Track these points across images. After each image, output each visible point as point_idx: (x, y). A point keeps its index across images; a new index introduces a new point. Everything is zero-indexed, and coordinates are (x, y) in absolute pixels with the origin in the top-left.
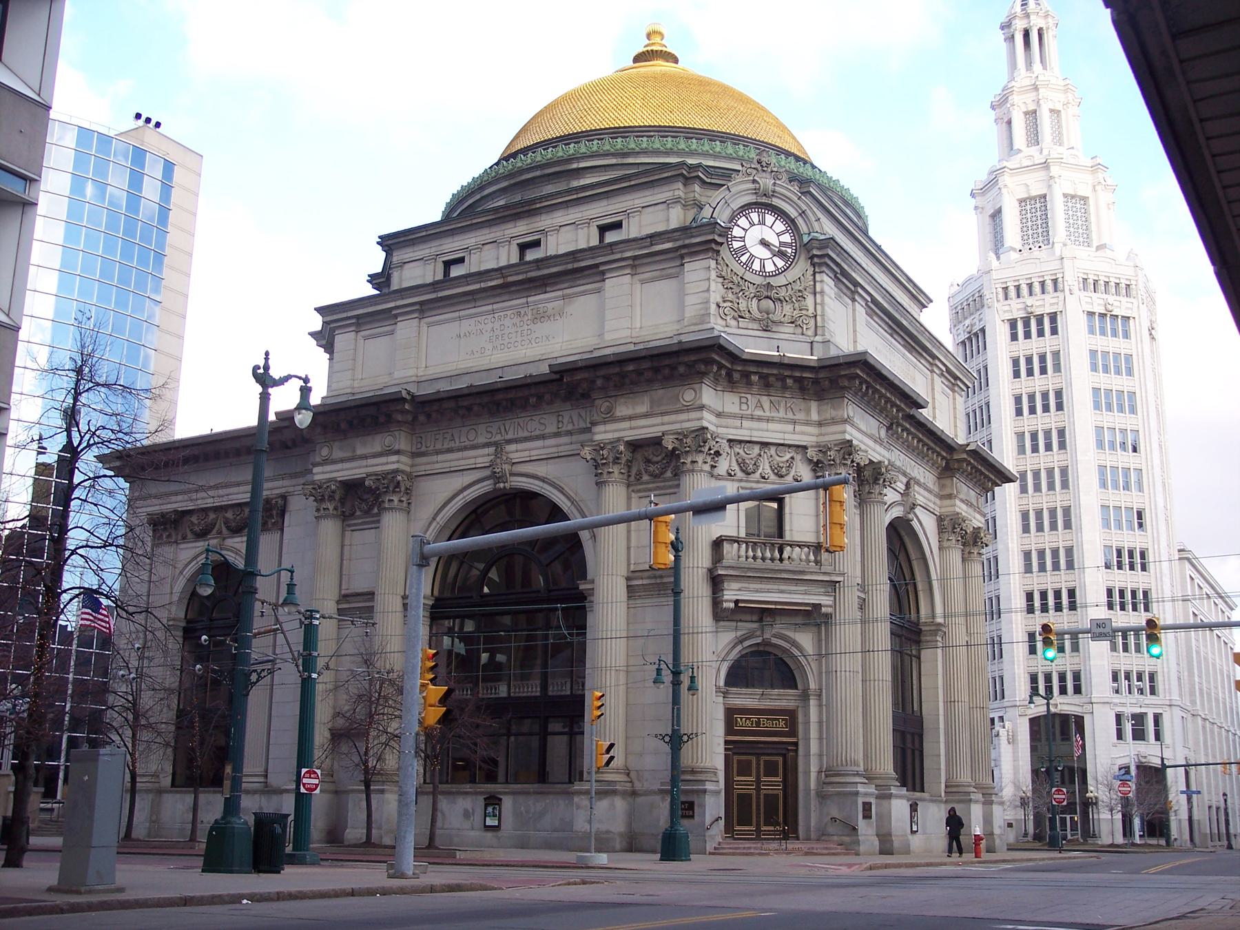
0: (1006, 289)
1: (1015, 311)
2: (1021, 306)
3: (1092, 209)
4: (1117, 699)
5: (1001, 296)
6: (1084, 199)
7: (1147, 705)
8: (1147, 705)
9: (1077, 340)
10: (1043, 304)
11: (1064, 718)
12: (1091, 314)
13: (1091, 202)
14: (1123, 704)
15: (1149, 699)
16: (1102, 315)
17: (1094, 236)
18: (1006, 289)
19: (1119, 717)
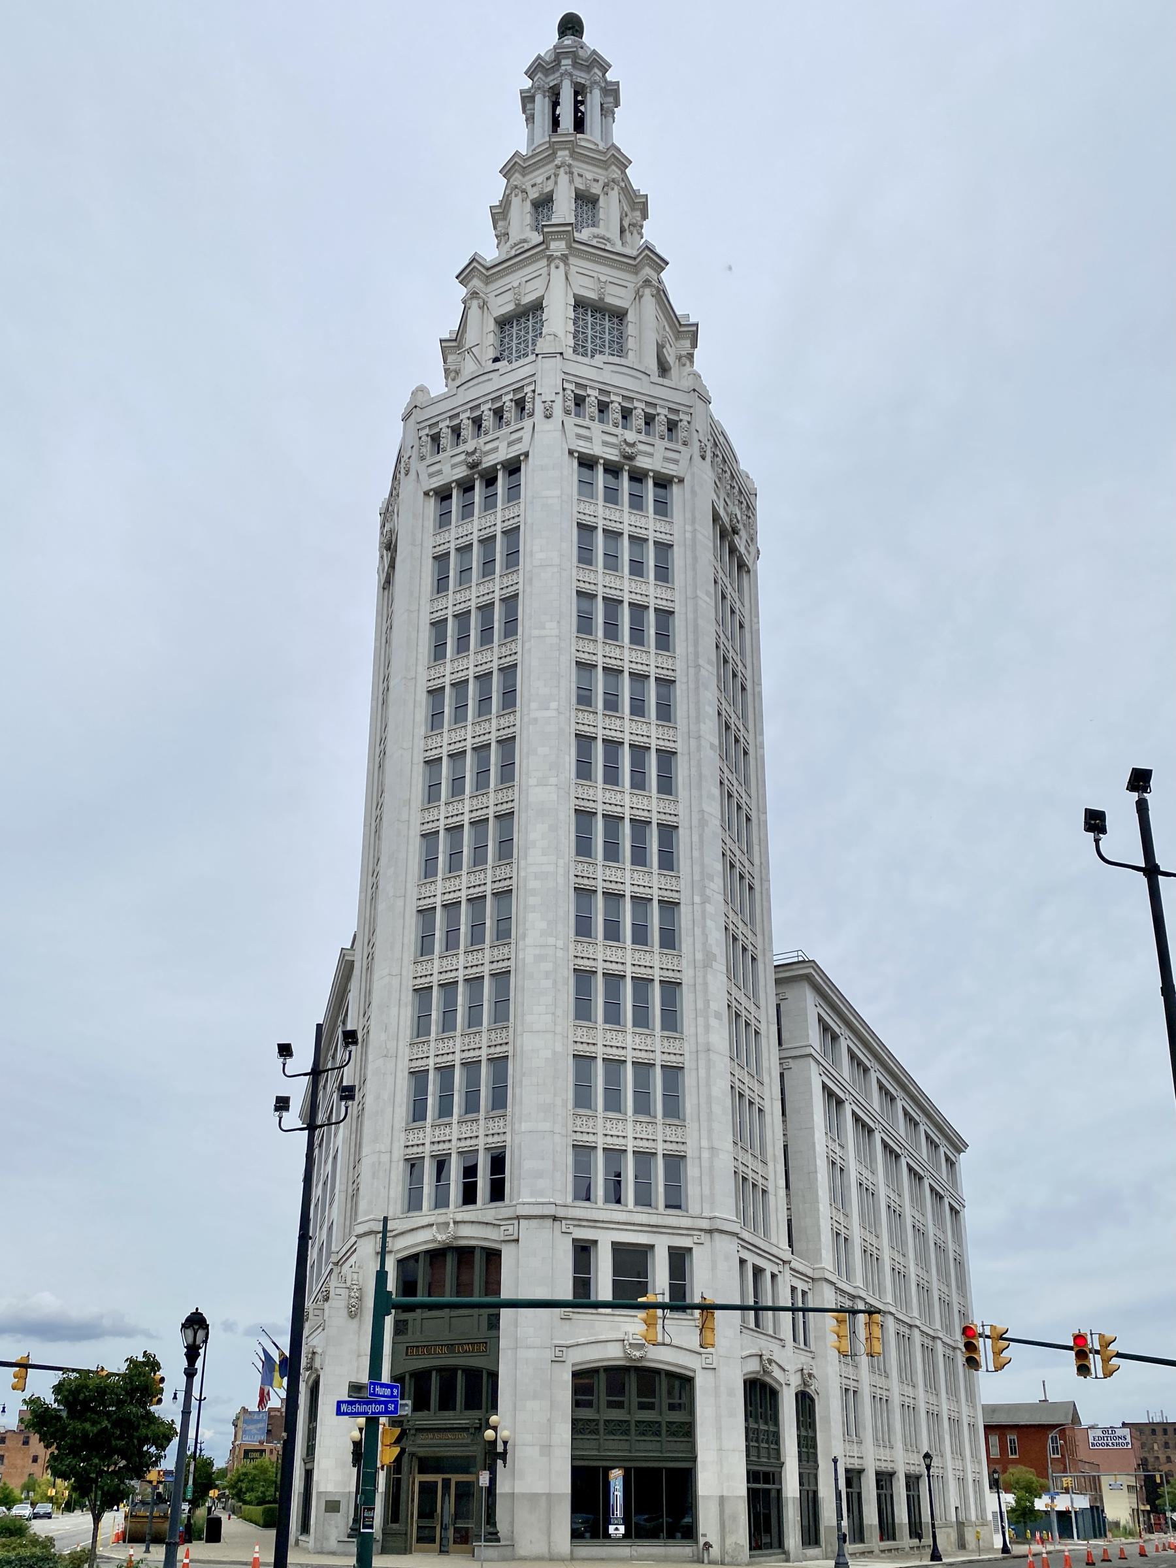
0: (436, 438)
1: (446, 469)
2: (463, 457)
3: (631, 330)
4: (582, 1210)
5: (428, 448)
6: (619, 315)
7: (655, 1228)
8: (655, 1228)
9: (549, 501)
10: (497, 450)
11: (464, 1254)
12: (587, 463)
13: (630, 317)
14: (594, 1223)
15: (660, 1215)
16: (613, 470)
18: (436, 438)
19: (583, 1251)
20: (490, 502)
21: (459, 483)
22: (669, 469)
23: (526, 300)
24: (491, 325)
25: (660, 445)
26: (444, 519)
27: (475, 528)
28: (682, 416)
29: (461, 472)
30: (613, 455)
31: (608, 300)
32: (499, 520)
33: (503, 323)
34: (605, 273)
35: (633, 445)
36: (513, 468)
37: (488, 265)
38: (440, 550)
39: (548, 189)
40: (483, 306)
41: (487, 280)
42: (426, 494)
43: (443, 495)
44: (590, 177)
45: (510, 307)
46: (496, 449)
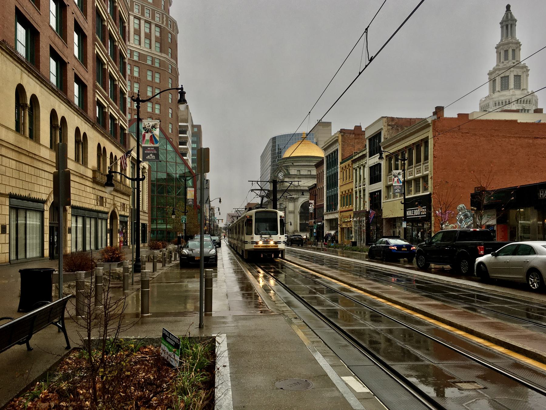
3: (522, 79)
17: (522, 86)
34: (518, 70)
44: (514, 46)
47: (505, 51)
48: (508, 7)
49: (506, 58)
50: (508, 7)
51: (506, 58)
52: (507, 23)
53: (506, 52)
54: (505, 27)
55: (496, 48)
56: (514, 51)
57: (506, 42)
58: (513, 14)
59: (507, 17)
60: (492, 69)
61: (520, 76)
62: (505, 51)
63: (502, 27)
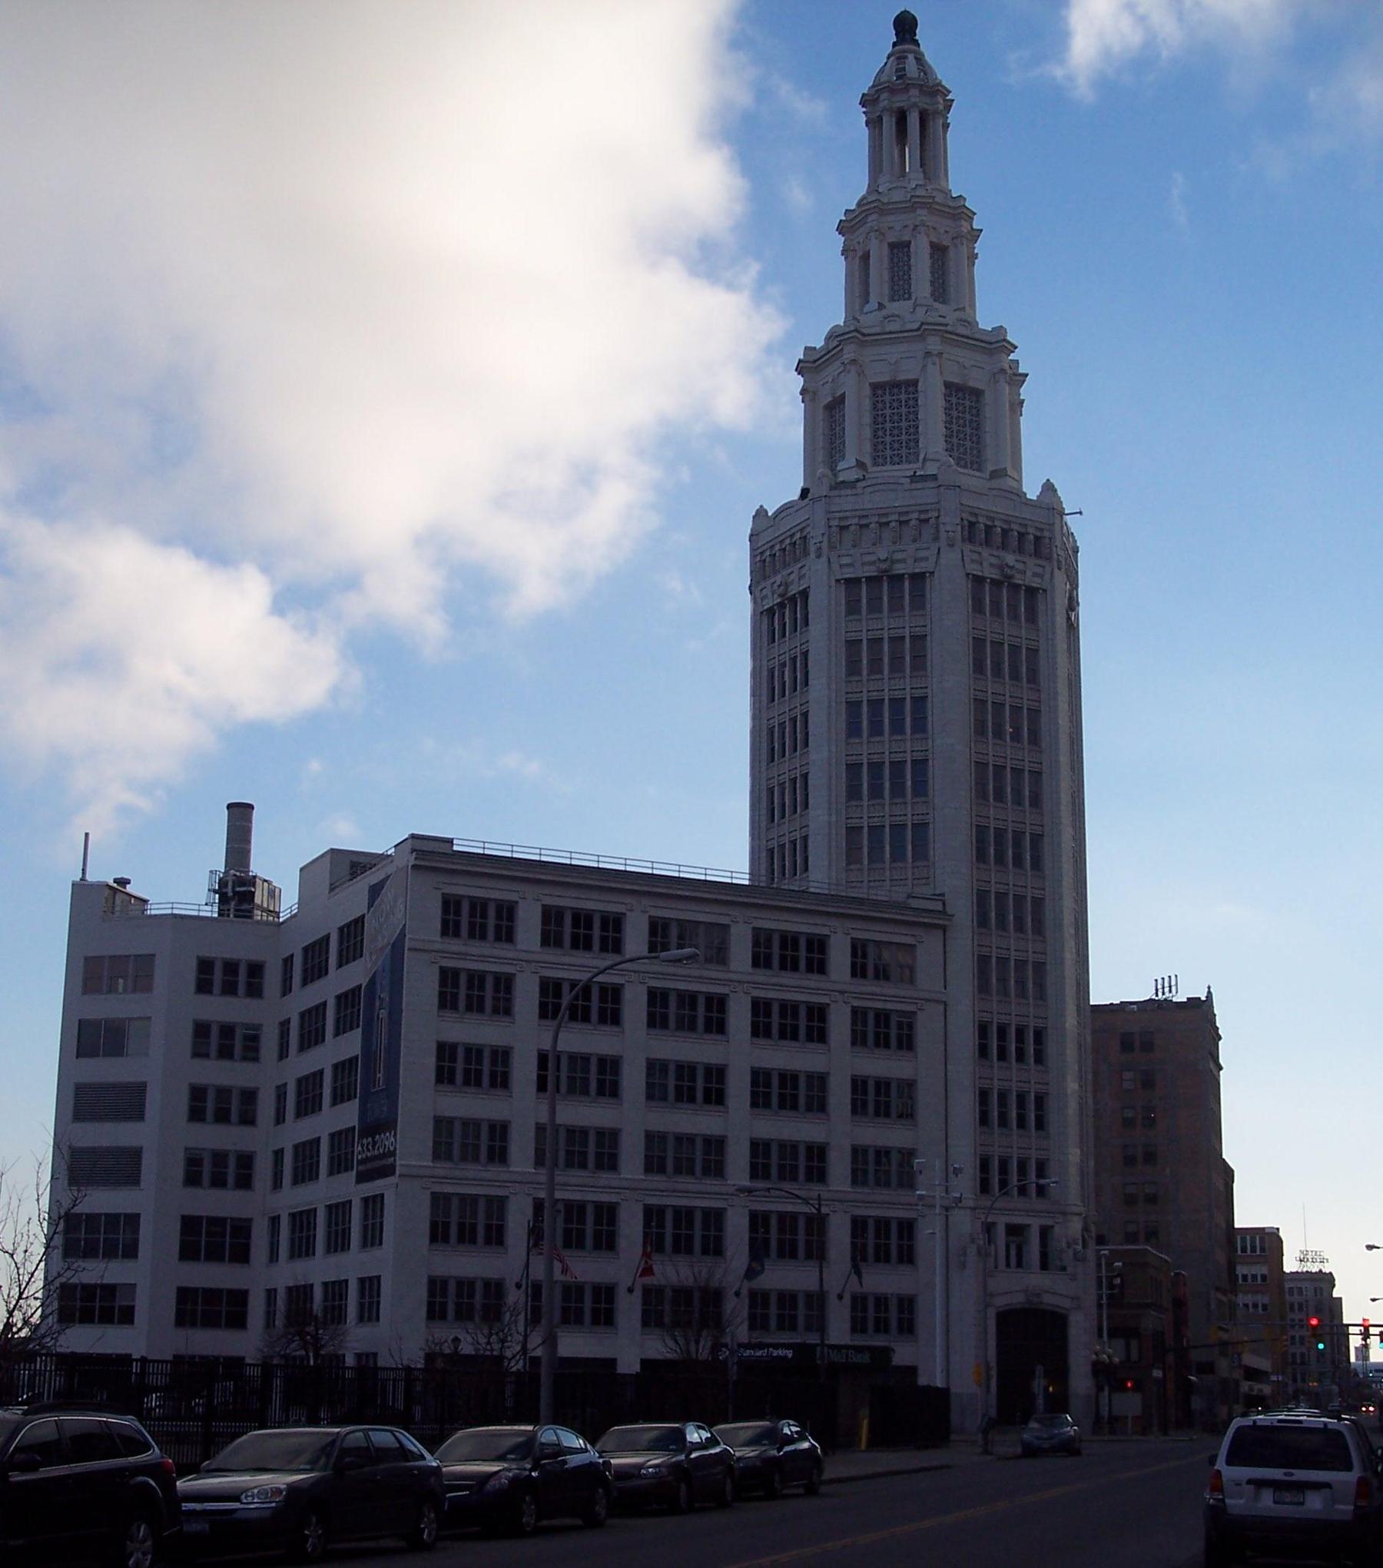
12: (978, 580)
17: (989, 453)
20: (896, 606)
21: (869, 579)
22: (1036, 583)
23: (902, 377)
24: (867, 391)
25: (1031, 562)
26: (852, 608)
27: (886, 624)
28: (1046, 534)
29: (871, 571)
30: (994, 574)
31: (971, 384)
32: (906, 624)
33: (875, 387)
35: (1012, 568)
36: (918, 578)
37: (865, 331)
38: (853, 636)
39: (906, 238)
40: (861, 374)
41: (863, 344)
42: (838, 581)
43: (851, 583)
45: (886, 378)
46: (904, 561)
47: (892, 246)
48: (905, 26)
49: (900, 287)
50: (905, 26)
51: (900, 287)
52: (900, 101)
53: (900, 250)
54: (889, 124)
55: (841, 229)
56: (939, 251)
57: (897, 196)
58: (929, 57)
59: (901, 73)
60: (819, 343)
61: (977, 394)
62: (892, 246)
63: (874, 123)
